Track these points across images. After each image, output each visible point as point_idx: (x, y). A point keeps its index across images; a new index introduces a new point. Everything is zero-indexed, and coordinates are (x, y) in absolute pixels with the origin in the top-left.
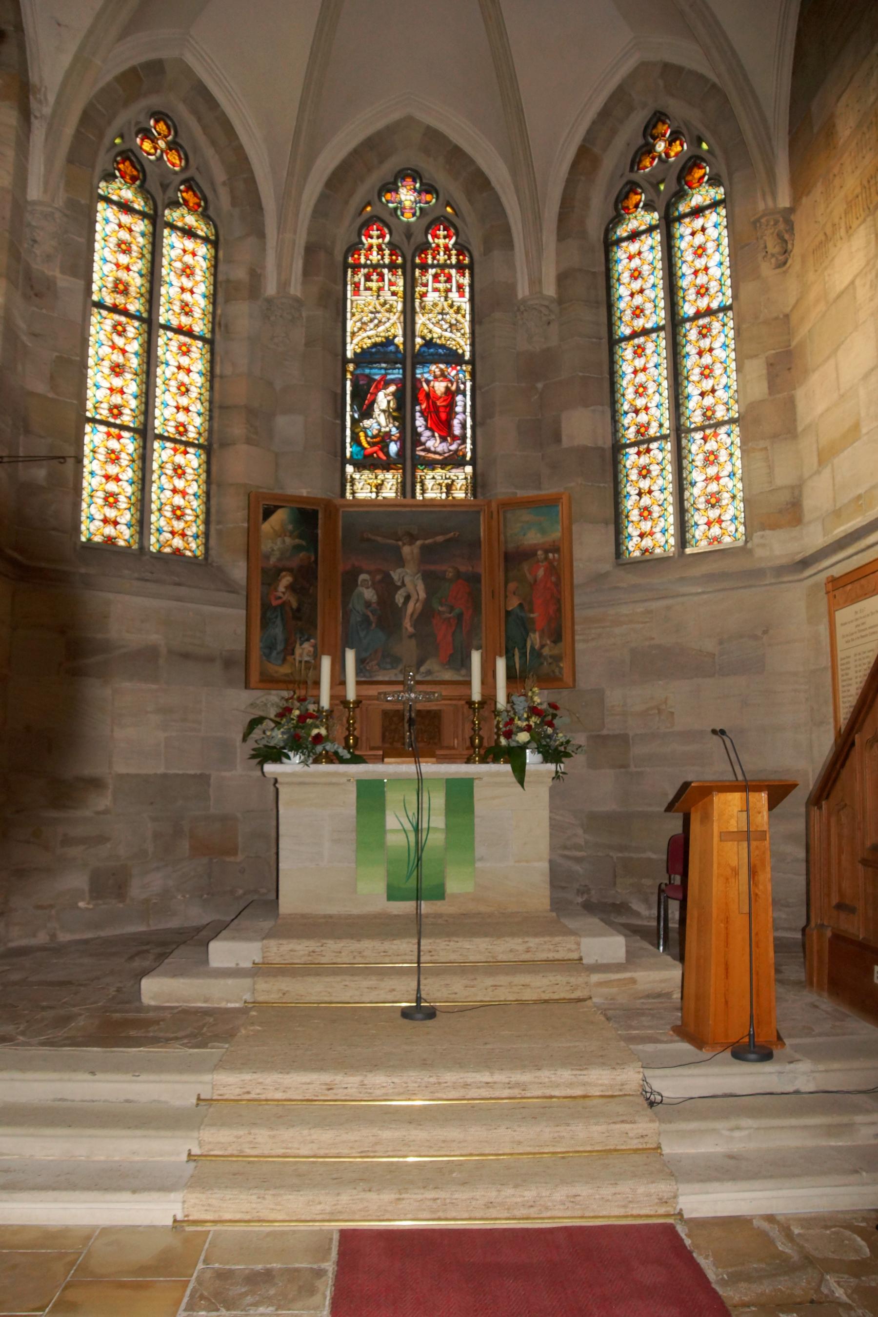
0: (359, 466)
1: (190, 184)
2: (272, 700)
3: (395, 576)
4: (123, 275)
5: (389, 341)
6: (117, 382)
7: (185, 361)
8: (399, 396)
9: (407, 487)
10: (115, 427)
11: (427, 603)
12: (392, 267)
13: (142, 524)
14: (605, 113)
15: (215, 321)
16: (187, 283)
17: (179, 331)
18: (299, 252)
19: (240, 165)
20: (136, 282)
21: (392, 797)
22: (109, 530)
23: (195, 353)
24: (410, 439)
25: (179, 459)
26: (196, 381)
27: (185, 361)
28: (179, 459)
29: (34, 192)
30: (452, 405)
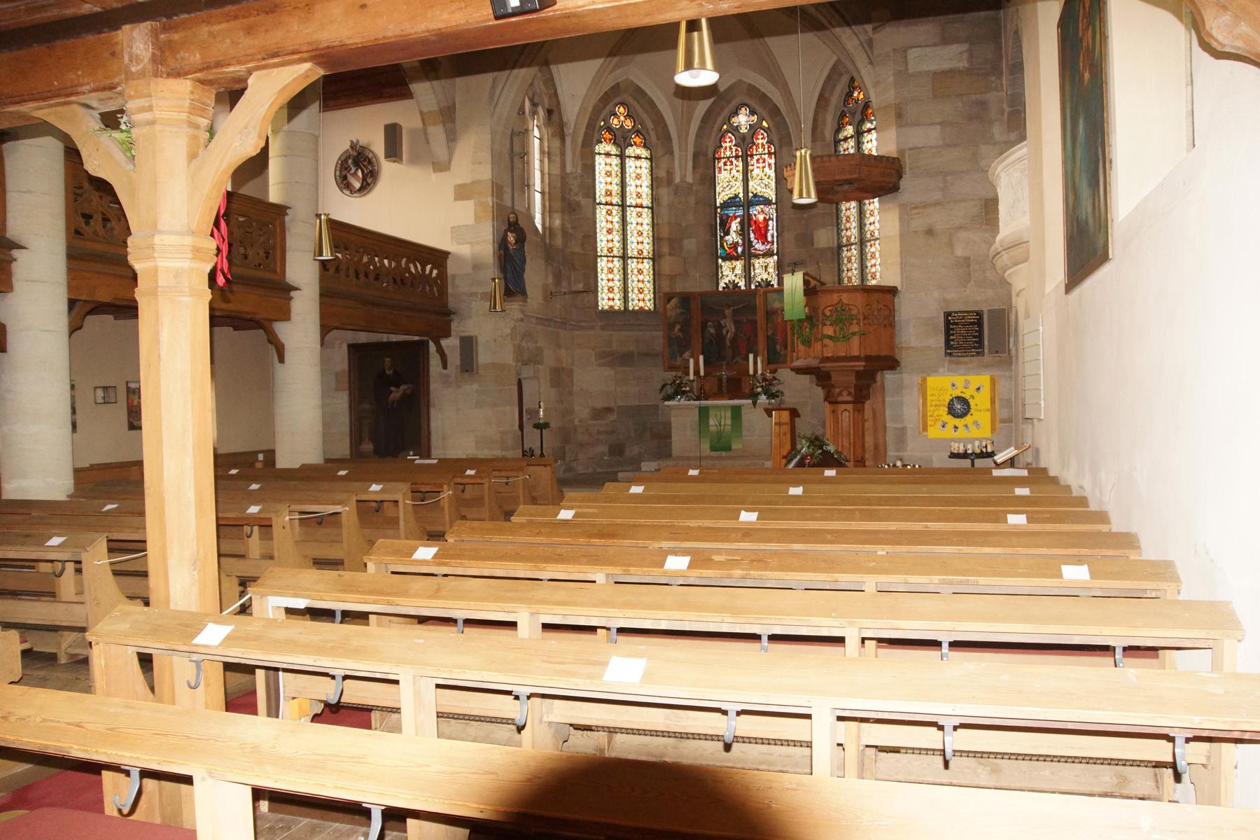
0: (724, 259)
1: (638, 133)
2: (670, 375)
3: (722, 322)
4: (609, 187)
5: (736, 196)
6: (610, 237)
7: (640, 220)
8: (741, 223)
9: (748, 268)
10: (610, 256)
11: (736, 335)
12: (737, 157)
13: (625, 299)
14: (829, 78)
15: (654, 199)
16: (638, 183)
17: (636, 206)
18: (690, 157)
19: (659, 119)
20: (615, 189)
21: (712, 412)
22: (611, 303)
23: (644, 215)
24: (748, 244)
25: (640, 266)
26: (646, 229)
27: (640, 220)
28: (640, 266)
29: (569, 169)
30: (767, 226)
